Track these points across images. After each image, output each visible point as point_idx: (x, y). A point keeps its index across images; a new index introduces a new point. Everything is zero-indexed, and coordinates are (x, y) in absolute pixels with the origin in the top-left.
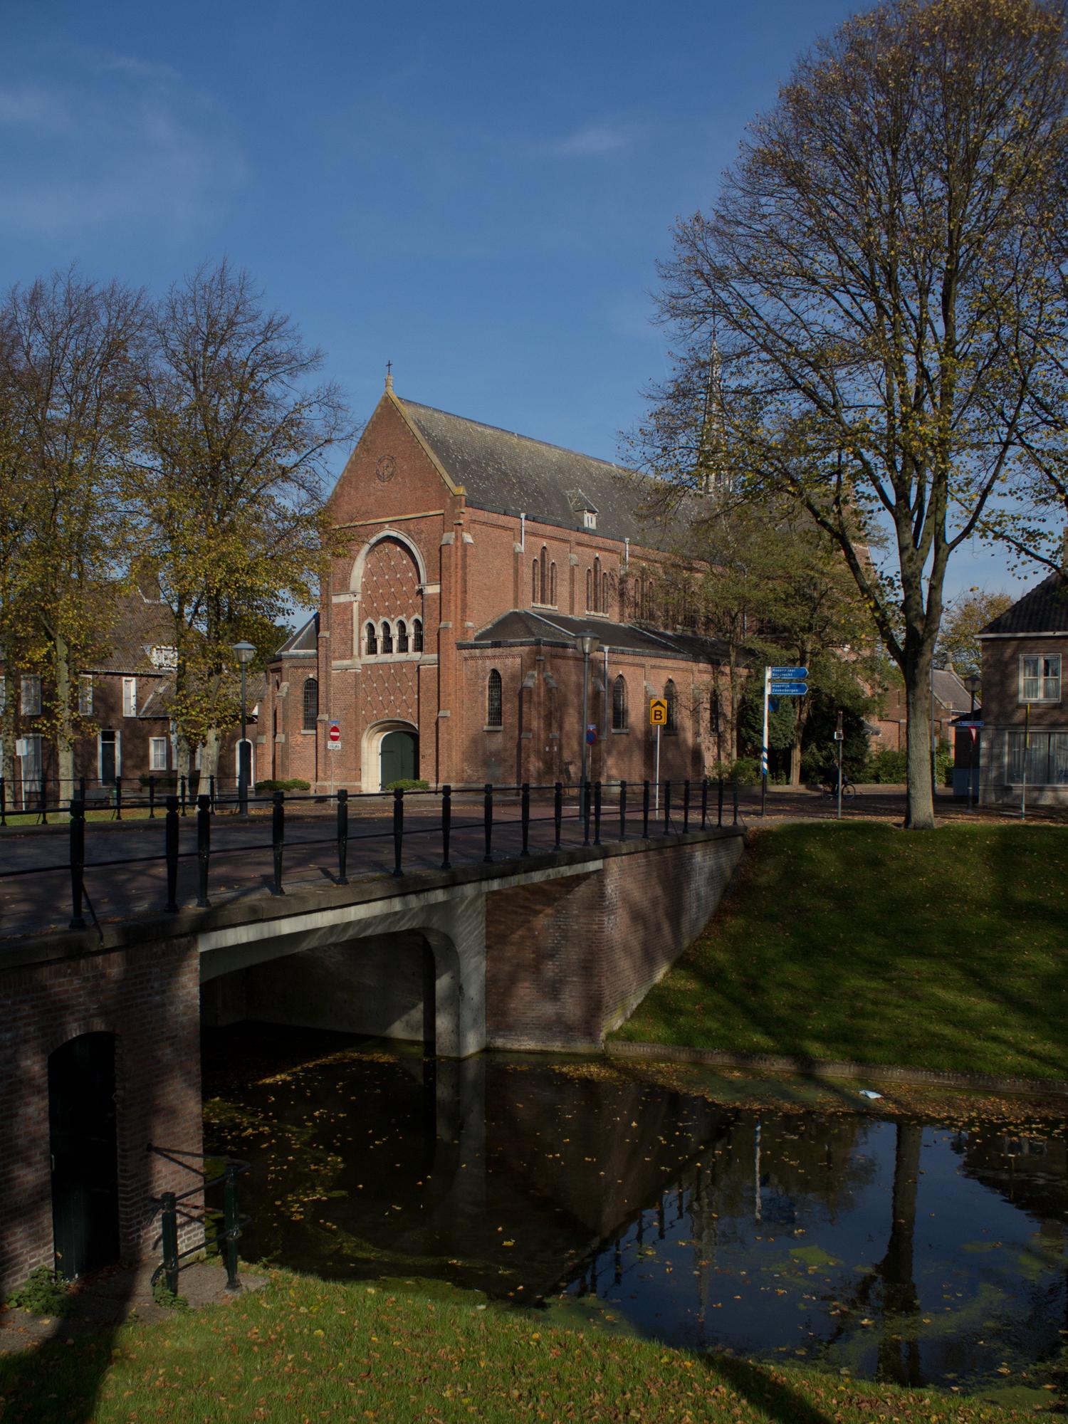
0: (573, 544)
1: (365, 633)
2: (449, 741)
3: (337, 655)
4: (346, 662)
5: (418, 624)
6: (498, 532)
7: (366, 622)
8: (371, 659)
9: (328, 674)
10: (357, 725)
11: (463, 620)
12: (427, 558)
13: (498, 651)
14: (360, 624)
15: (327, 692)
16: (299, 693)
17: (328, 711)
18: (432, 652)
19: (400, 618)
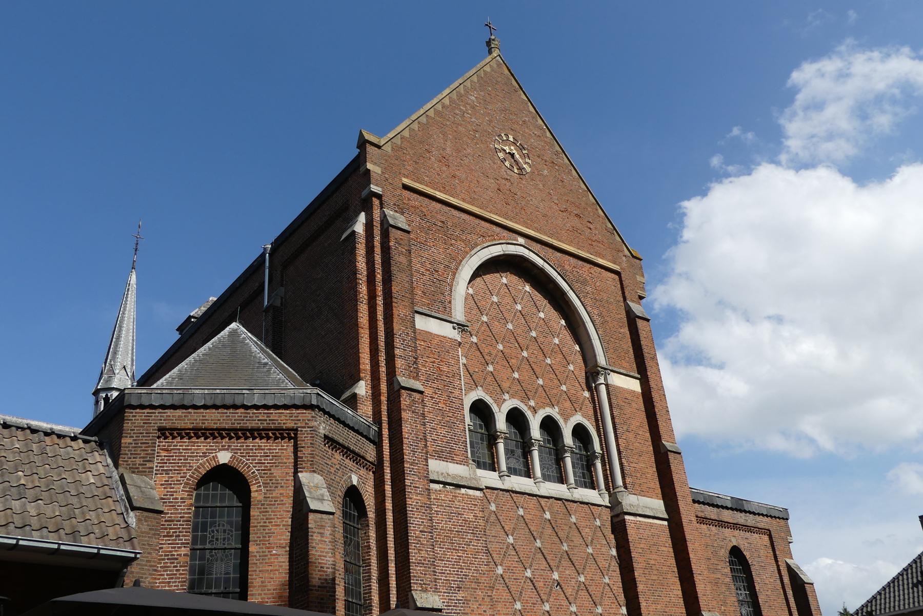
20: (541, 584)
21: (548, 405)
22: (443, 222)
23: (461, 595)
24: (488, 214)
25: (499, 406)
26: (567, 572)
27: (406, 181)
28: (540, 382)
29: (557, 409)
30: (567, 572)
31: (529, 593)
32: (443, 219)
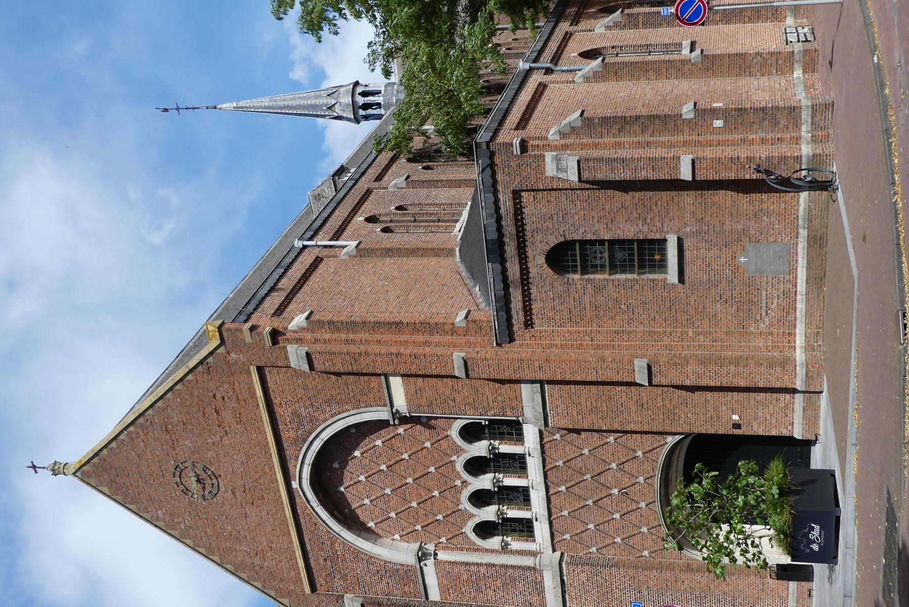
0: (377, 184)
1: (495, 542)
2: (702, 362)
4: (550, 582)
5: (471, 433)
6: (314, 279)
7: (473, 537)
8: (541, 530)
10: (671, 567)
11: (454, 330)
12: (341, 403)
13: (511, 249)
14: (478, 550)
18: (518, 398)
19: (459, 467)
22: (325, 560)
23: (646, 593)
24: (289, 520)
26: (610, 479)
27: (307, 590)
28: (432, 469)
29: (454, 458)
30: (610, 479)
31: (633, 517)
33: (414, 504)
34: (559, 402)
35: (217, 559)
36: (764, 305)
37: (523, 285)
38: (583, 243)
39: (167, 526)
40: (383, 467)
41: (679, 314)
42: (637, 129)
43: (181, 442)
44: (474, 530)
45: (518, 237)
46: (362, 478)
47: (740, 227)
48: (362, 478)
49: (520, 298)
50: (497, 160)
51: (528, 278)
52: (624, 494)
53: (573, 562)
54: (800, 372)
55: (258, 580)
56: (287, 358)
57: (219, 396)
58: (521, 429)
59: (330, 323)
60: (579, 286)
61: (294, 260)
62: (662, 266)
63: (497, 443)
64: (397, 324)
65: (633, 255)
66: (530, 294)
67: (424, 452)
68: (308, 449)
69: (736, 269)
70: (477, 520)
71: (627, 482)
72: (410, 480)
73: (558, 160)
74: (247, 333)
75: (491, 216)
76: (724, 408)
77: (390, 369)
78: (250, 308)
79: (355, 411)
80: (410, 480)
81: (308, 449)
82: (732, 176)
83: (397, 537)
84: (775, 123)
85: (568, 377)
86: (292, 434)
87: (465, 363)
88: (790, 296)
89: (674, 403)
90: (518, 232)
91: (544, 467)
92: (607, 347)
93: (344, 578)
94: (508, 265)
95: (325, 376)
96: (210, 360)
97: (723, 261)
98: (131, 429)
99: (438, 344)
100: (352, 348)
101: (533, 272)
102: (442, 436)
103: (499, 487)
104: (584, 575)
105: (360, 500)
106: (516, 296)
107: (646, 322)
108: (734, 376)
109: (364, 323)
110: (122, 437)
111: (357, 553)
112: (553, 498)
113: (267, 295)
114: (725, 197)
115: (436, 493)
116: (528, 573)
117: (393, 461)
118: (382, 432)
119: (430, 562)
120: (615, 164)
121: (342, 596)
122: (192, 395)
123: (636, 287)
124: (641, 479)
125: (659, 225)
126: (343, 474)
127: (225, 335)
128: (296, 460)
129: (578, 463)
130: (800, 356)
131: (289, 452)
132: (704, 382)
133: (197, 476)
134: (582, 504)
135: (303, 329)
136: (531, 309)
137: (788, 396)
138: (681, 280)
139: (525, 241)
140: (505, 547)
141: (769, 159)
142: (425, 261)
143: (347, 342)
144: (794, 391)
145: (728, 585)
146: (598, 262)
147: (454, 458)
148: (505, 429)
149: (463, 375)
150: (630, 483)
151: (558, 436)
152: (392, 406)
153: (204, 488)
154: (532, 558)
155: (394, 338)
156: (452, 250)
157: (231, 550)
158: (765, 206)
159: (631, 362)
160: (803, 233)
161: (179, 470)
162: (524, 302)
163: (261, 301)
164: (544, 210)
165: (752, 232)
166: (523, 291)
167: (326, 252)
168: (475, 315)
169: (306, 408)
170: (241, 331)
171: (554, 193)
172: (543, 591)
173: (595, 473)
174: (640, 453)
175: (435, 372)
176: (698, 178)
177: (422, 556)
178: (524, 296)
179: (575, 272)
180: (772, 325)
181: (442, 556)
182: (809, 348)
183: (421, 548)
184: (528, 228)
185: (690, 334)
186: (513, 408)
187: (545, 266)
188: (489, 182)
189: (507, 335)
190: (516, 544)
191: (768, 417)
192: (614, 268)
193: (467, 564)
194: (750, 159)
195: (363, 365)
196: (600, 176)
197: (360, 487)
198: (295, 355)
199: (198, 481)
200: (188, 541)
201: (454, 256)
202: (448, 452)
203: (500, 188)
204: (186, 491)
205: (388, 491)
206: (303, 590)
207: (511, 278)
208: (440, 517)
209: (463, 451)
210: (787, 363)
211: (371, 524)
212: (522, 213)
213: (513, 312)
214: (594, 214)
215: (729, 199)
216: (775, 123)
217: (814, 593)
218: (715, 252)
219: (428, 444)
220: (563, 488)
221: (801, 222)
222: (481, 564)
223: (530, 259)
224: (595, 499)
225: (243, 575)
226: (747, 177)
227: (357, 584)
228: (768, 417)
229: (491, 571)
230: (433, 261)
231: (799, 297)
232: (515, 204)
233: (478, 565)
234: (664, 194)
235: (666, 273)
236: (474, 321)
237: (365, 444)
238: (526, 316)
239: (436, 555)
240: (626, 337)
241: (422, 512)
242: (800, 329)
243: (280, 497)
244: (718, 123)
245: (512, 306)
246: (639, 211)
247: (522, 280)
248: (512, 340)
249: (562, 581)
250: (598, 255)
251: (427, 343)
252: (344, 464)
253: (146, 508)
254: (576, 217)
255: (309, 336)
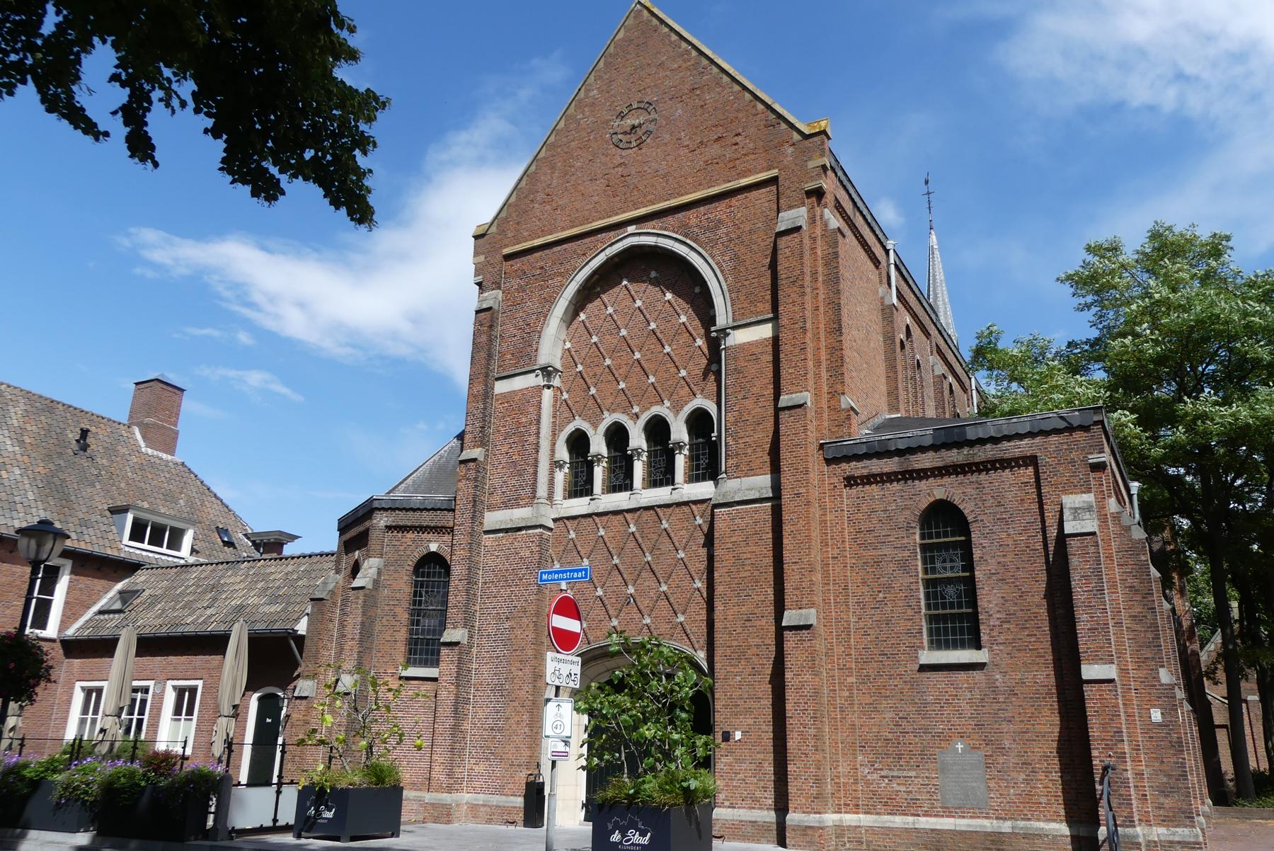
1: (563, 454)
2: (817, 693)
3: (497, 499)
4: (519, 515)
7: (570, 428)
8: (580, 505)
9: (473, 545)
11: (834, 394)
13: (954, 456)
14: (554, 435)
15: (470, 580)
16: (402, 584)
17: (468, 623)
18: (751, 472)
19: (656, 410)
20: (613, 600)
21: (657, 403)
25: (595, 426)
26: (647, 584)
27: (507, 251)
28: (652, 379)
29: (667, 403)
30: (647, 584)
31: (598, 612)
32: (542, 264)
33: (608, 362)
34: (747, 520)
35: (542, 154)
36: (895, 774)
37: (903, 473)
38: (967, 548)
39: (580, 101)
40: (653, 326)
41: (875, 665)
42: (1137, 609)
43: (679, 105)
44: (578, 430)
45: (970, 465)
46: (639, 303)
47: (1007, 744)
48: (639, 303)
49: (886, 470)
50: (1078, 435)
51: (914, 479)
52: (628, 600)
53: (542, 542)
54: (812, 819)
55: (518, 199)
56: (790, 207)
57: (738, 139)
58: (704, 479)
59: (836, 255)
60: (905, 541)
61: (876, 236)
62: (938, 642)
63: (686, 452)
64: (840, 329)
65: (952, 607)
66: (891, 482)
67: (673, 370)
68: (676, 240)
69: (946, 738)
70: (590, 432)
71: (644, 603)
72: (637, 355)
73: (1089, 509)
74: (820, 162)
75: (1000, 431)
76: (751, 721)
77: (784, 320)
78: (840, 173)
79: (725, 287)
80: (637, 355)
81: (676, 240)
82: (1095, 731)
83: (568, 345)
84: (1164, 791)
85: (787, 528)
86: (693, 221)
87: (800, 406)
88: (911, 808)
89: (755, 659)
90: (977, 464)
91: (659, 506)
92: (826, 575)
93: (521, 289)
94: (931, 454)
95: (769, 252)
96: (784, 126)
97: (955, 720)
98: (694, 53)
99: (818, 376)
100: (808, 278)
101: (922, 485)
102: (695, 389)
103: (631, 457)
104: (528, 553)
105: (612, 302)
106: (890, 465)
107: (862, 625)
108: (801, 734)
109: (838, 292)
110: (684, 45)
111: (550, 301)
112: (620, 517)
113: (850, 195)
114: (1049, 723)
115: (622, 385)
116: (528, 490)
117: (660, 336)
118: (697, 322)
119: (541, 381)
120: (1094, 580)
121: (499, 288)
122: (738, 111)
123: (910, 612)
124: (647, 621)
125: (1002, 638)
126: (644, 282)
127: (816, 139)
128: (661, 228)
129: (666, 545)
130: (830, 818)
131: (670, 220)
132: (790, 696)
133: (640, 125)
134: (613, 552)
135: (826, 225)
136: (870, 483)
137: (770, 802)
138: (924, 668)
139: (965, 473)
140: (557, 465)
141: (1125, 782)
142: (883, 380)
143: (814, 274)
144: (782, 807)
145: (518, 723)
146: (938, 565)
147: (667, 403)
148: (704, 462)
149: (781, 405)
150: (642, 607)
151: (699, 521)
152: (734, 328)
153: (625, 133)
154: (545, 495)
155: (822, 326)
156: (898, 410)
157: (553, 168)
158: (1041, 776)
159: (812, 605)
160: (1006, 827)
161: (646, 107)
162: (881, 475)
163: (844, 187)
164: (1009, 496)
165: (1001, 759)
166: (896, 473)
167: (884, 274)
168: (855, 420)
169: (727, 235)
170: (822, 155)
171: (1035, 507)
172: (507, 507)
173: (653, 566)
174: (681, 618)
175: (783, 373)
176: (1086, 687)
177: (547, 371)
178: (888, 475)
179: (923, 537)
180: (868, 783)
181: (547, 395)
182: (840, 830)
183: (556, 371)
184: (983, 476)
185: (850, 680)
186: (737, 466)
187: (932, 499)
188: (1047, 426)
189: (835, 456)
190: (561, 477)
191: (741, 776)
192: (928, 583)
193: (538, 421)
194: (1122, 756)
195: (788, 291)
196: (1074, 561)
197: (628, 302)
198: (796, 215)
199: (634, 127)
200: (562, 124)
201: (890, 411)
202: (675, 397)
203: (1038, 440)
204: (621, 116)
205: (624, 332)
206: (506, 246)
207: (912, 458)
208: (593, 391)
209: (677, 413)
210: (818, 802)
211: (582, 316)
212: (1003, 469)
213: (866, 462)
214: (1010, 557)
215: (1046, 729)
216: (1164, 791)
217: (512, 828)
218: (967, 710)
219: (683, 373)
220: (633, 529)
221: (1022, 824)
222: (538, 437)
223: (939, 481)
224: (620, 567)
225: (523, 183)
226: (1095, 753)
227: (513, 303)
228: (741, 776)
229: (530, 449)
230: (883, 388)
231: (910, 819)
232: (1016, 460)
233: (538, 433)
234: (1048, 645)
235: (930, 648)
236: (848, 417)
237: (680, 304)
238: (862, 477)
239: (549, 387)
240: (841, 598)
241: (599, 372)
242: (865, 820)
243: (617, 214)
244: (1156, 715)
245: (875, 461)
246: (1019, 614)
247: (911, 472)
248: (829, 462)
249: (520, 529)
250: (948, 565)
251: (818, 363)
252: (655, 283)
253: (601, 77)
254: (1004, 535)
255: (818, 232)
